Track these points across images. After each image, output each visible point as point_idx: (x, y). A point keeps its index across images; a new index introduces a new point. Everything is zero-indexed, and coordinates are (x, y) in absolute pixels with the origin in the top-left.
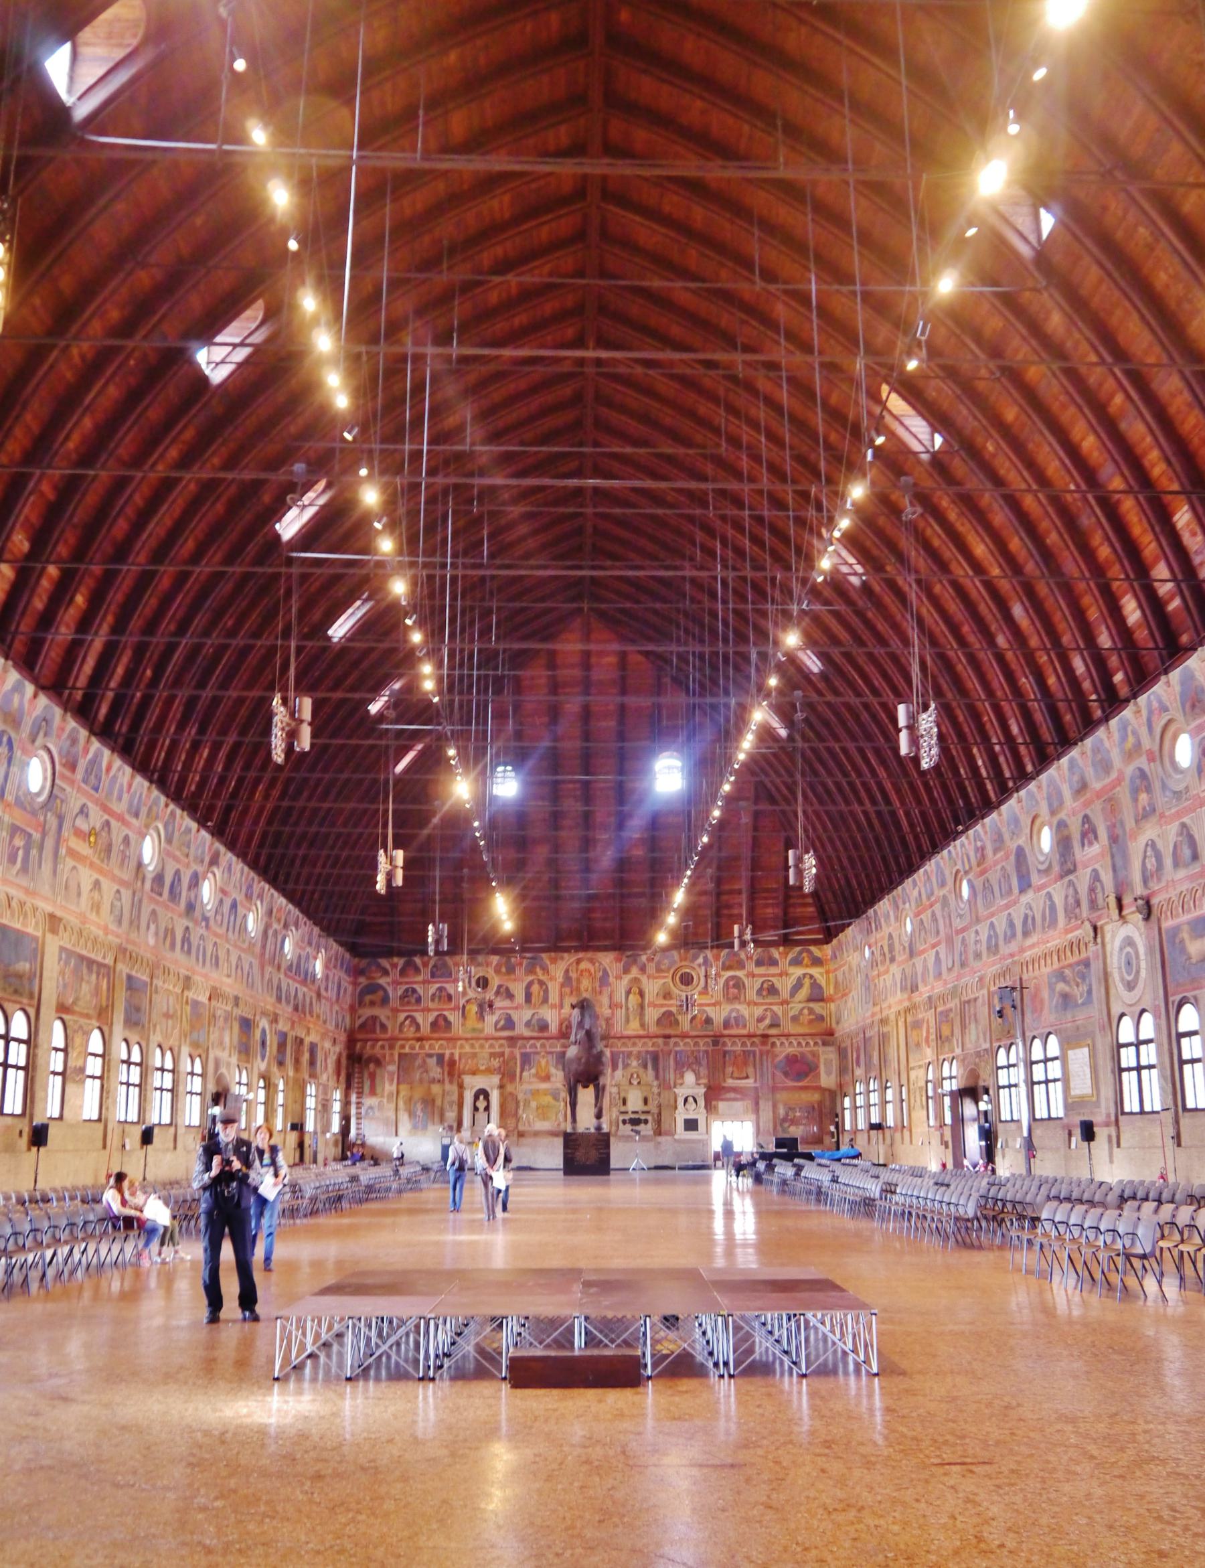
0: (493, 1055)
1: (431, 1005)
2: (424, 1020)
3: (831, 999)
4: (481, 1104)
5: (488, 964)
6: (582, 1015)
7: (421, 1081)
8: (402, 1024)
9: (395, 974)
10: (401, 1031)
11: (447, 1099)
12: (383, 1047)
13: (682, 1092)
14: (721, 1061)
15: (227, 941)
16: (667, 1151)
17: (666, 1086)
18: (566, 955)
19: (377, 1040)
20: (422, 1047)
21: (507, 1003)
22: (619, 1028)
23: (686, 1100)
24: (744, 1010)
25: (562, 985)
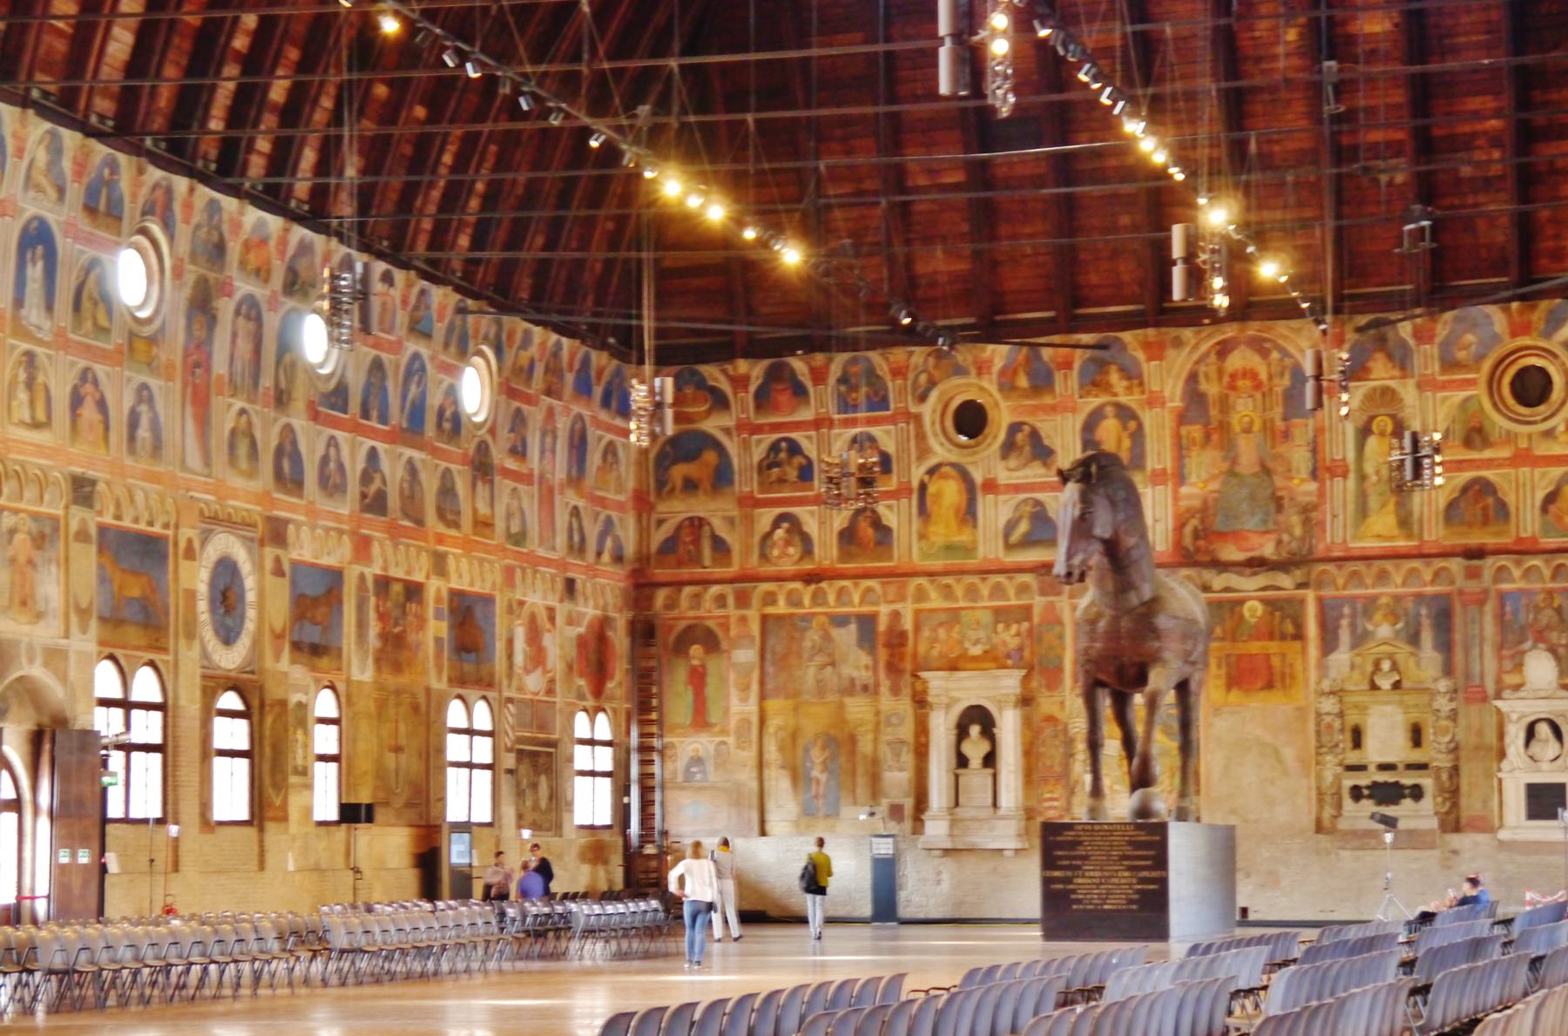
0: (1001, 615)
2: (823, 525)
4: (975, 749)
5: (982, 368)
6: (1085, 499)
7: (821, 690)
8: (768, 535)
9: (743, 405)
10: (764, 556)
11: (887, 735)
12: (721, 600)
13: (1519, 710)
15: (26, 335)
17: (1474, 694)
18: (1188, 333)
19: (706, 582)
20: (818, 598)
21: (1036, 473)
22: (1338, 533)
25: (1182, 419)
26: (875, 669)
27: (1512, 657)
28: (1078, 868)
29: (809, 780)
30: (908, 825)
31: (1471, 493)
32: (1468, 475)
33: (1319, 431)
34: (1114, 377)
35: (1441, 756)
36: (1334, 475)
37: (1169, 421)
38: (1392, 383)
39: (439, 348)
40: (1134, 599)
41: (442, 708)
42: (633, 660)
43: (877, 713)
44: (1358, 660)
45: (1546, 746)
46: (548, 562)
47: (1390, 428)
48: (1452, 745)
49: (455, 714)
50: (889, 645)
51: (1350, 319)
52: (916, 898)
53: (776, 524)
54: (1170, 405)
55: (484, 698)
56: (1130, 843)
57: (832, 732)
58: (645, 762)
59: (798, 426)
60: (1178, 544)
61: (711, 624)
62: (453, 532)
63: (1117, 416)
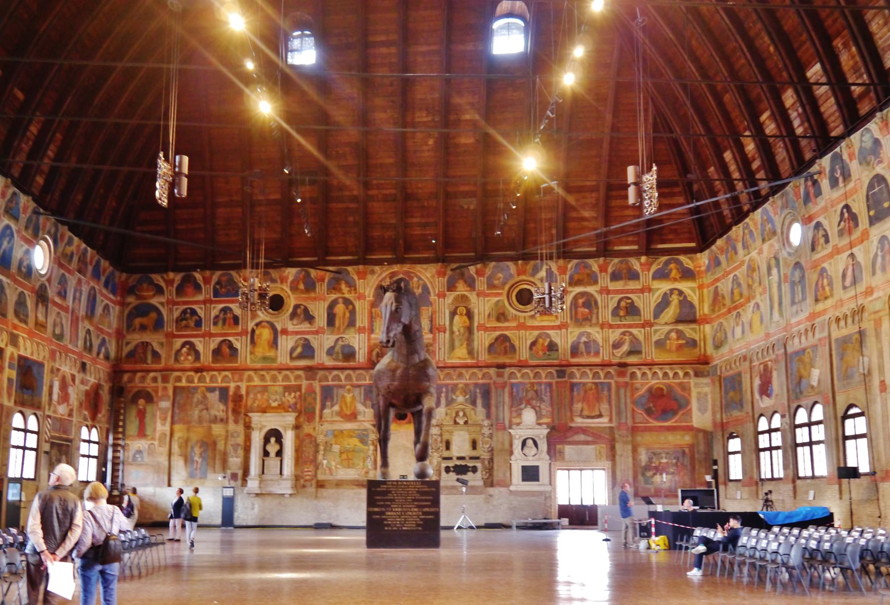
0: (287, 389)
1: (213, 330)
2: (205, 347)
3: (706, 320)
4: (273, 448)
5: (283, 280)
6: (398, 300)
7: (200, 420)
8: (179, 351)
9: (170, 293)
10: (177, 360)
11: (231, 441)
12: (155, 380)
13: (518, 434)
14: (567, 399)
16: (500, 506)
17: (500, 426)
18: (377, 268)
19: (148, 371)
21: (305, 326)
23: (524, 443)
24: (596, 333)
26: (227, 412)
28: (389, 506)
29: (193, 461)
30: (239, 482)
32: (498, 333)
33: (433, 313)
34: (343, 286)
36: (439, 331)
37: (367, 306)
38: (466, 293)
39: (23, 228)
40: (416, 359)
41: (9, 416)
42: (111, 405)
43: (227, 432)
44: (449, 411)
45: (530, 449)
46: (73, 352)
47: (465, 312)
49: (17, 420)
50: (234, 401)
52: (242, 516)
53: (183, 346)
55: (35, 414)
56: (418, 492)
57: (205, 440)
58: (115, 451)
59: (196, 302)
61: (149, 390)
62: (23, 325)
63: (344, 303)
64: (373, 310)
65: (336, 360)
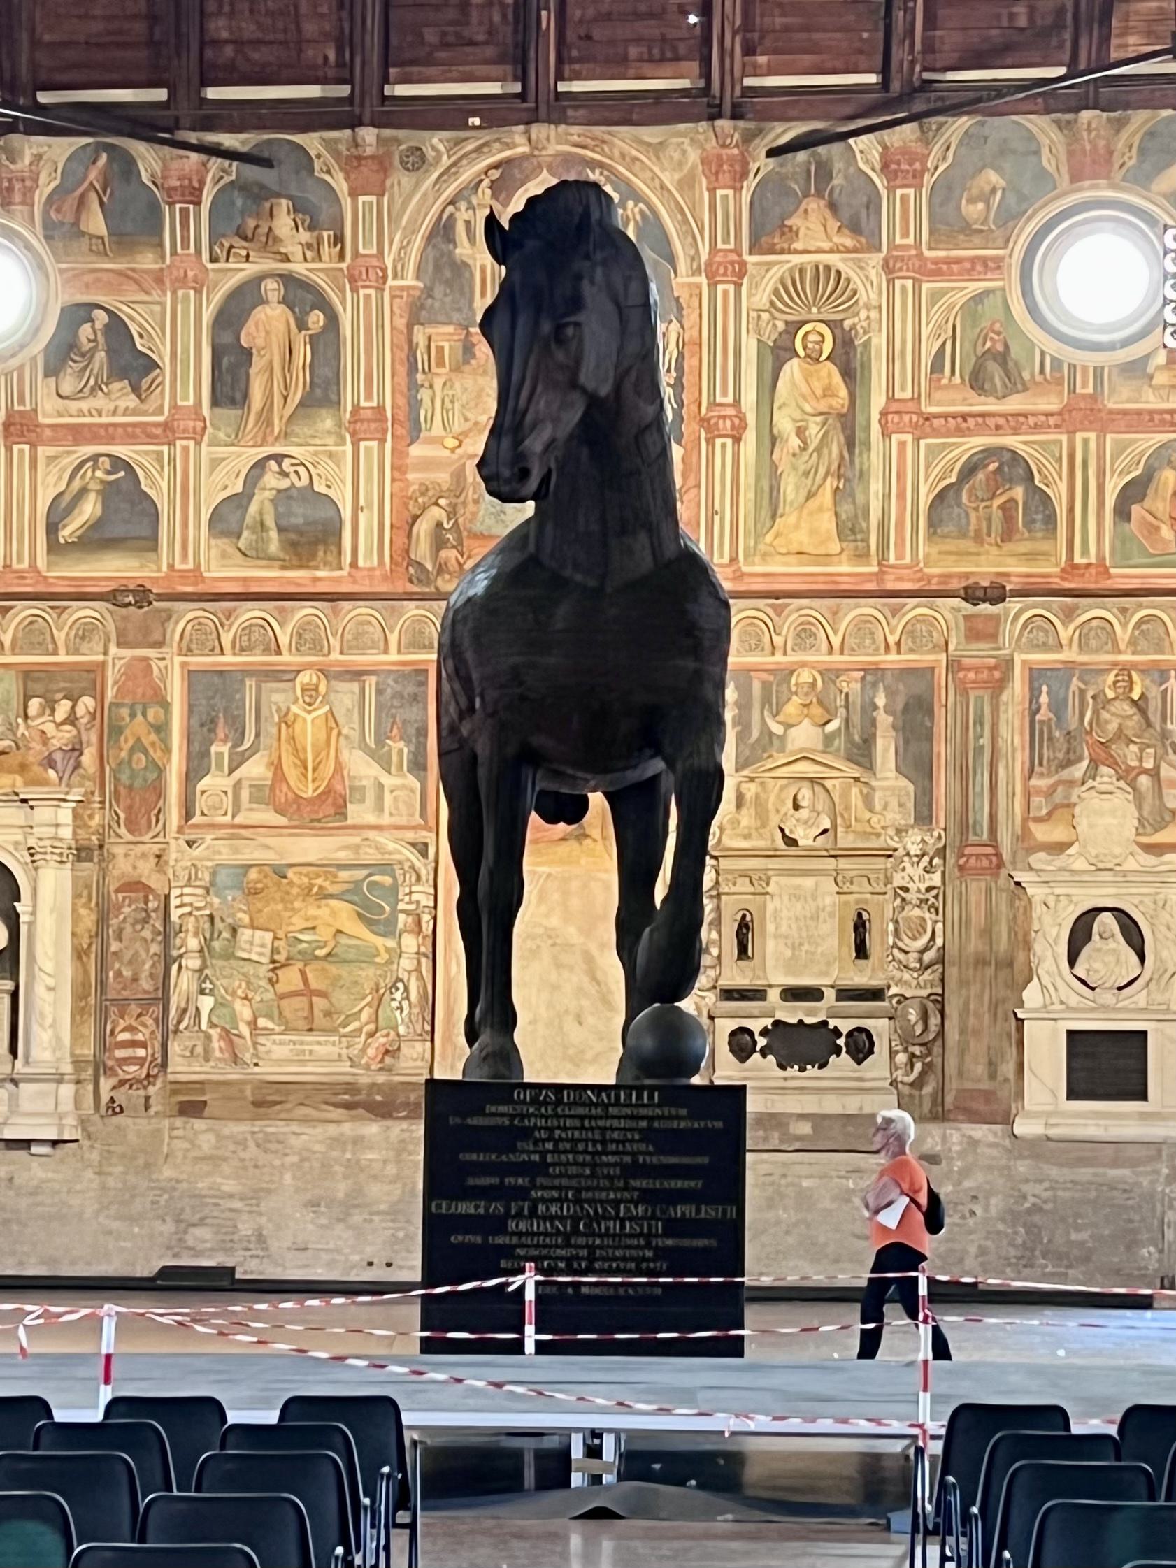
18: (436, 141)
21: (116, 404)
25: (417, 313)
27: (1051, 791)
28: (522, 1193)
31: (981, 476)
34: (283, 223)
35: (906, 976)
37: (393, 317)
38: (834, 260)
48: (928, 957)
51: (759, 132)
54: (390, 282)
56: (647, 1135)
60: (403, 556)
63: (284, 301)
64: (419, 335)
65: (256, 554)
